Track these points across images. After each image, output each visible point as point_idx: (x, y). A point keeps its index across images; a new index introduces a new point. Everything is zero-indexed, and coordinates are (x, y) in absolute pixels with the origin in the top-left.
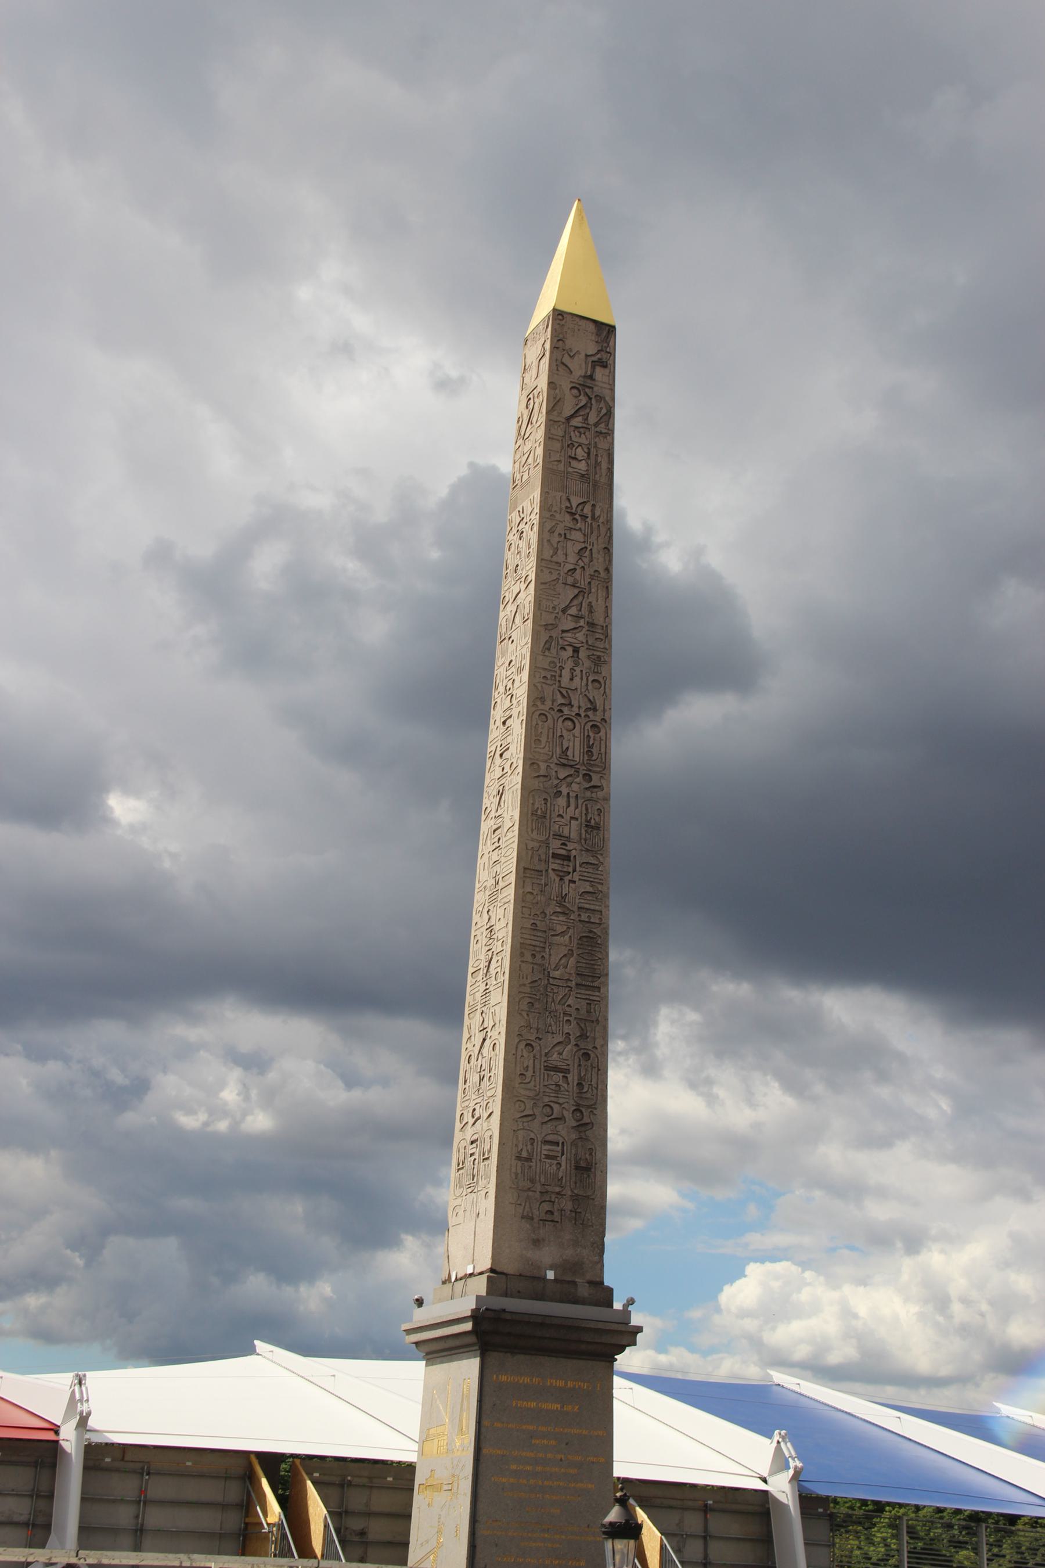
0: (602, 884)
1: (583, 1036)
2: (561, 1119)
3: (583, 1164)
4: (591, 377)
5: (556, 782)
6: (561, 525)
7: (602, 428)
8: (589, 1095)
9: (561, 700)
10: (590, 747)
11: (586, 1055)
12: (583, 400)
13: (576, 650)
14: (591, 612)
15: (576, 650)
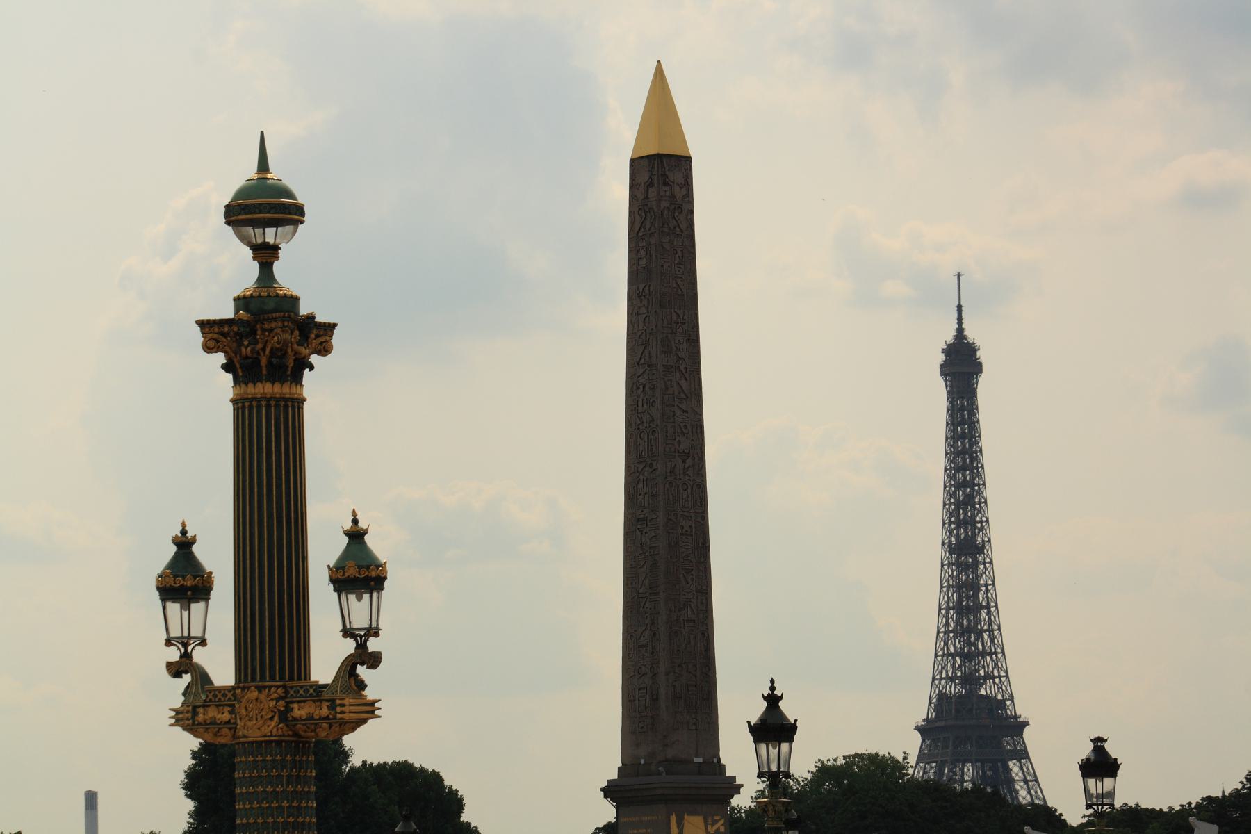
0: (658, 529)
1: (653, 623)
2: (646, 674)
3: (655, 697)
4: (647, 198)
5: (638, 474)
6: (636, 308)
7: (652, 231)
8: (656, 657)
9: (638, 422)
10: (651, 446)
11: (654, 634)
12: (643, 214)
13: (644, 387)
14: (650, 357)
15: (644, 387)
